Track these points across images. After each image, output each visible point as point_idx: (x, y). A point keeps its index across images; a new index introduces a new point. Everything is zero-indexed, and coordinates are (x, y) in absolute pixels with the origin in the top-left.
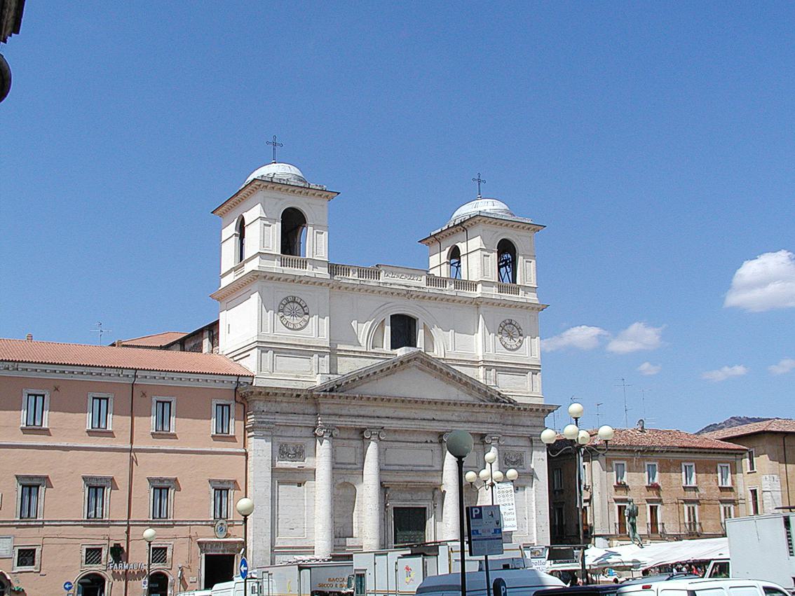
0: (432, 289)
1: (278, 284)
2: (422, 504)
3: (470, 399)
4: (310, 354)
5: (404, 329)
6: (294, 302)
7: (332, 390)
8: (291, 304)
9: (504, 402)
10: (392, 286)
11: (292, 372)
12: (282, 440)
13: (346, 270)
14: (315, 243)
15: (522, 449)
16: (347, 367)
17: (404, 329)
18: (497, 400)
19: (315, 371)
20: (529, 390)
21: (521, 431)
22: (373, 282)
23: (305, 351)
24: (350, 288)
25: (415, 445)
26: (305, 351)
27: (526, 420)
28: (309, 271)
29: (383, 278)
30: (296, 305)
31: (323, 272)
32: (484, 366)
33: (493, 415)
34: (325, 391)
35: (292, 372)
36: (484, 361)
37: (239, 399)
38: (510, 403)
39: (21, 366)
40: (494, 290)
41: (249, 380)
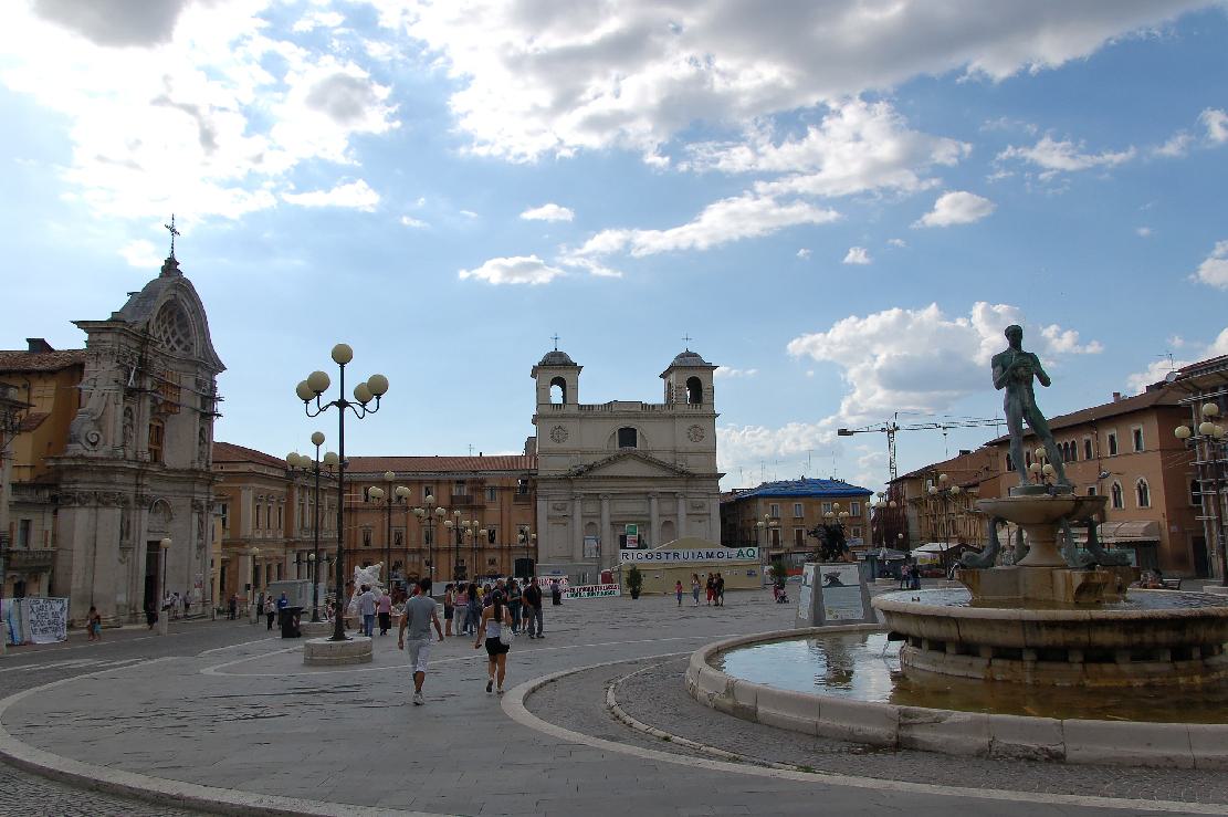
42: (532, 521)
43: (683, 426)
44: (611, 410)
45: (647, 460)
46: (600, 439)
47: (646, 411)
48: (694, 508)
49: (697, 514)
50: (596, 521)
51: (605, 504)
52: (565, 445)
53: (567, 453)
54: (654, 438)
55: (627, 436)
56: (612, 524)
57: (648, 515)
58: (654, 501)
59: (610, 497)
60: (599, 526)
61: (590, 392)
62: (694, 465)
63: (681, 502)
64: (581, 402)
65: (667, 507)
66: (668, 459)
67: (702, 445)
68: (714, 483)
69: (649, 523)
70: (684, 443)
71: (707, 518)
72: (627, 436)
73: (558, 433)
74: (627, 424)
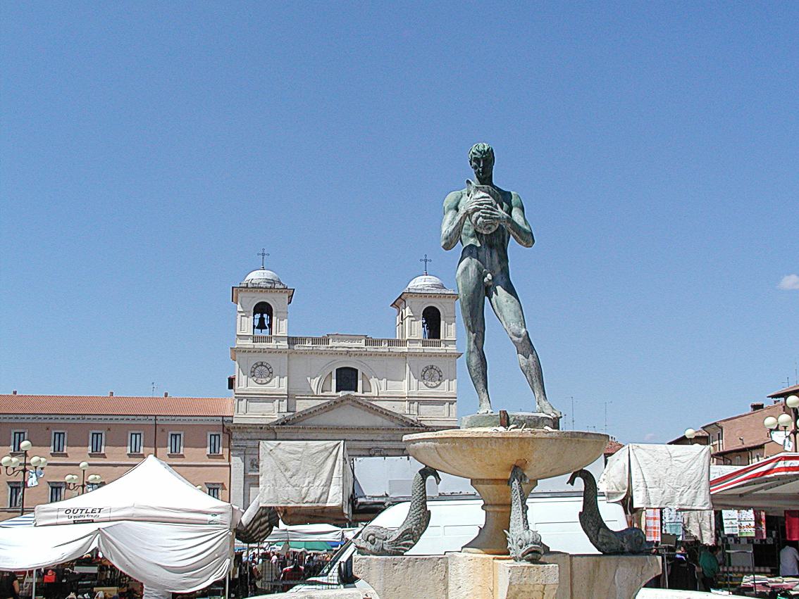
0: (370, 348)
1: (250, 354)
4: (273, 400)
5: (347, 378)
6: (262, 365)
7: (283, 424)
9: (417, 426)
10: (338, 349)
11: (260, 412)
13: (303, 340)
14: (281, 327)
16: (302, 406)
17: (347, 378)
18: (412, 425)
19: (277, 410)
20: (446, 415)
22: (322, 347)
23: (269, 398)
24: (305, 353)
26: (269, 398)
28: (273, 345)
29: (331, 344)
30: (263, 368)
31: (284, 344)
32: (408, 401)
34: (278, 424)
35: (260, 412)
36: (408, 397)
38: (422, 426)
39: (86, 417)
40: (419, 345)
41: (230, 419)
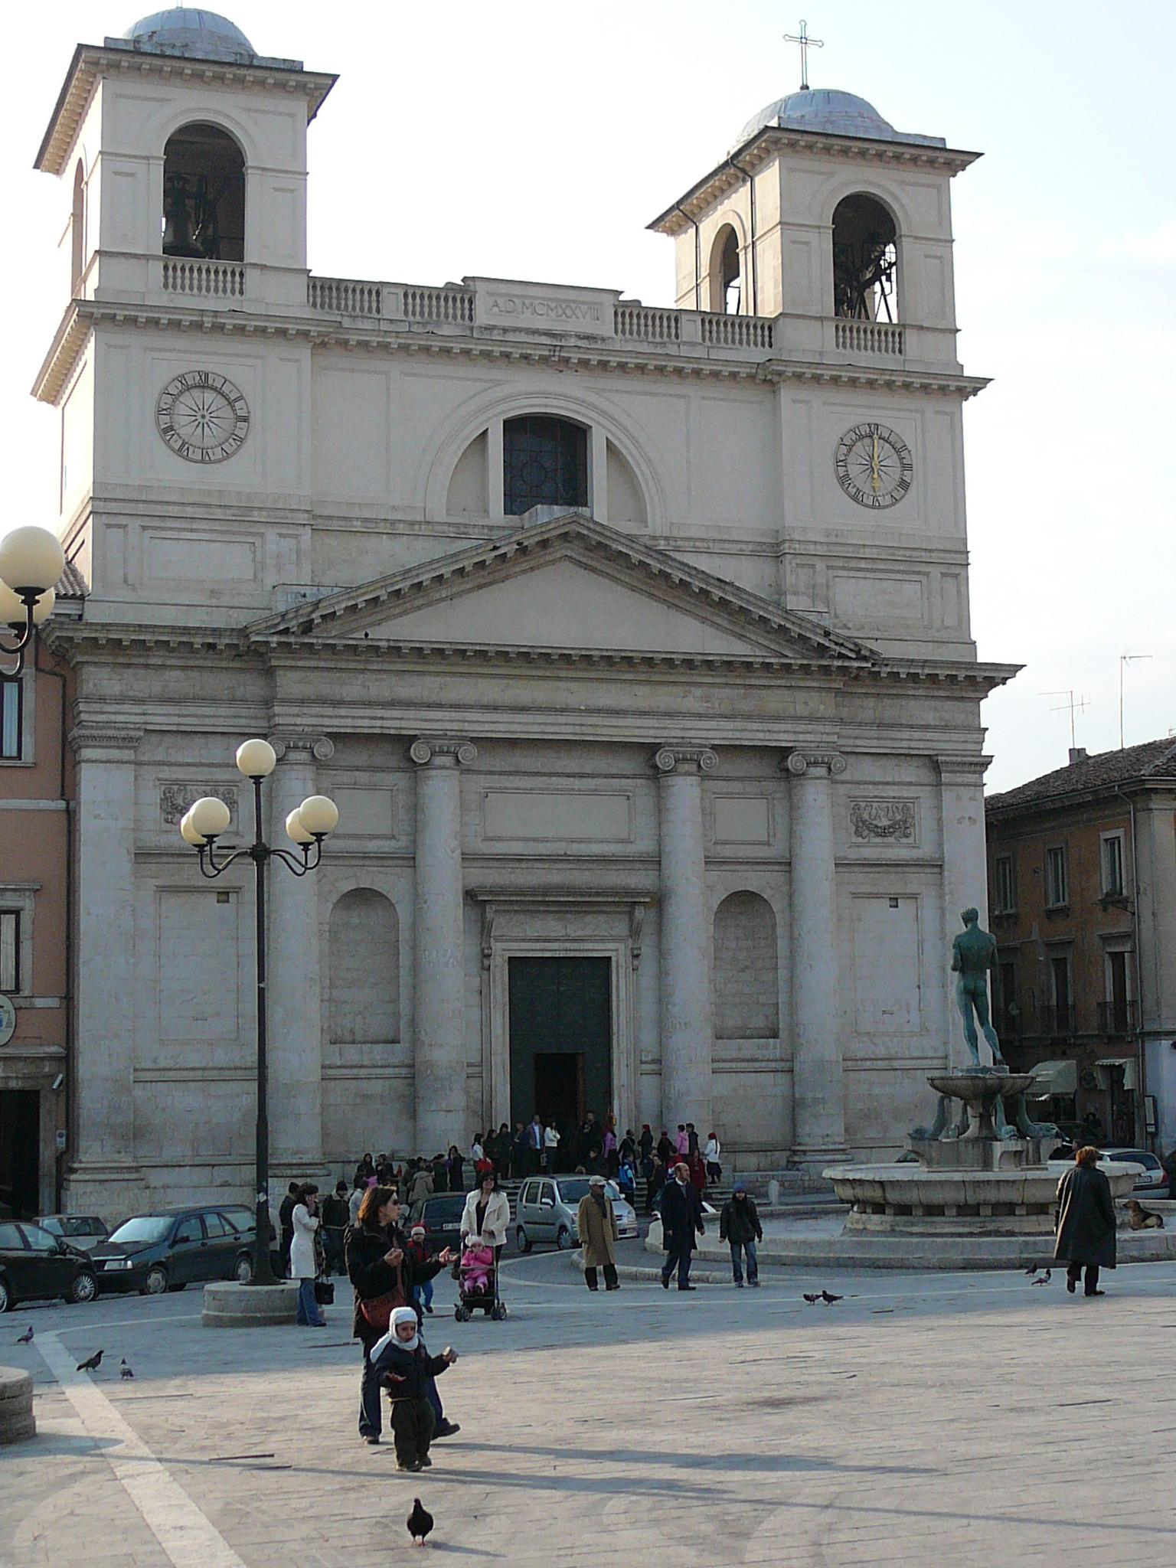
1: (153, 339)
2: (597, 950)
3: (738, 649)
7: (308, 627)
8: (196, 393)
9: (841, 656)
10: (510, 337)
12: (167, 773)
15: (912, 792)
18: (822, 650)
21: (905, 739)
25: (577, 783)
27: (923, 710)
30: (209, 396)
33: (813, 700)
34: (286, 631)
37: (48, 663)
38: (865, 659)
42: (221, 741)
43: (814, 423)
44: (448, 322)
45: (654, 573)
46: (410, 458)
47: (631, 339)
48: (864, 827)
49: (886, 859)
50: (390, 882)
51: (442, 790)
52: (237, 477)
53: (240, 519)
54: (685, 471)
55: (547, 456)
56: (472, 897)
57: (656, 861)
58: (685, 791)
59: (469, 753)
60: (403, 912)
61: (363, 210)
62: (858, 607)
63: (815, 795)
64: (323, 262)
65: (746, 819)
66: (747, 576)
67: (903, 523)
68: (952, 712)
69: (658, 900)
70: (817, 509)
71: (917, 881)
72: (547, 456)
73: (201, 419)
74: (545, 412)
